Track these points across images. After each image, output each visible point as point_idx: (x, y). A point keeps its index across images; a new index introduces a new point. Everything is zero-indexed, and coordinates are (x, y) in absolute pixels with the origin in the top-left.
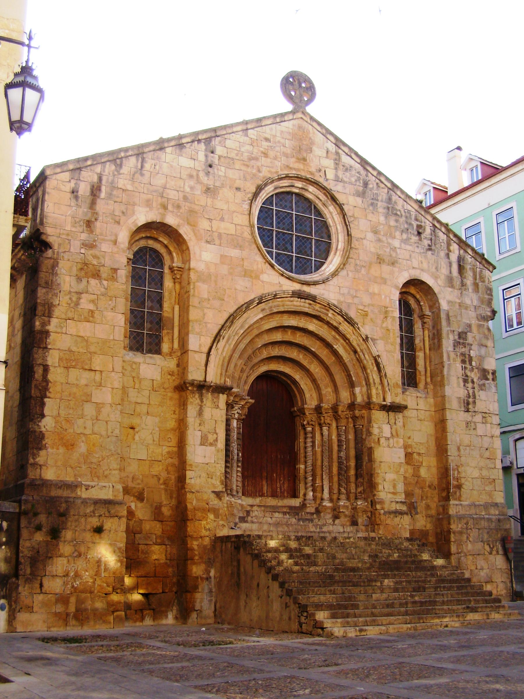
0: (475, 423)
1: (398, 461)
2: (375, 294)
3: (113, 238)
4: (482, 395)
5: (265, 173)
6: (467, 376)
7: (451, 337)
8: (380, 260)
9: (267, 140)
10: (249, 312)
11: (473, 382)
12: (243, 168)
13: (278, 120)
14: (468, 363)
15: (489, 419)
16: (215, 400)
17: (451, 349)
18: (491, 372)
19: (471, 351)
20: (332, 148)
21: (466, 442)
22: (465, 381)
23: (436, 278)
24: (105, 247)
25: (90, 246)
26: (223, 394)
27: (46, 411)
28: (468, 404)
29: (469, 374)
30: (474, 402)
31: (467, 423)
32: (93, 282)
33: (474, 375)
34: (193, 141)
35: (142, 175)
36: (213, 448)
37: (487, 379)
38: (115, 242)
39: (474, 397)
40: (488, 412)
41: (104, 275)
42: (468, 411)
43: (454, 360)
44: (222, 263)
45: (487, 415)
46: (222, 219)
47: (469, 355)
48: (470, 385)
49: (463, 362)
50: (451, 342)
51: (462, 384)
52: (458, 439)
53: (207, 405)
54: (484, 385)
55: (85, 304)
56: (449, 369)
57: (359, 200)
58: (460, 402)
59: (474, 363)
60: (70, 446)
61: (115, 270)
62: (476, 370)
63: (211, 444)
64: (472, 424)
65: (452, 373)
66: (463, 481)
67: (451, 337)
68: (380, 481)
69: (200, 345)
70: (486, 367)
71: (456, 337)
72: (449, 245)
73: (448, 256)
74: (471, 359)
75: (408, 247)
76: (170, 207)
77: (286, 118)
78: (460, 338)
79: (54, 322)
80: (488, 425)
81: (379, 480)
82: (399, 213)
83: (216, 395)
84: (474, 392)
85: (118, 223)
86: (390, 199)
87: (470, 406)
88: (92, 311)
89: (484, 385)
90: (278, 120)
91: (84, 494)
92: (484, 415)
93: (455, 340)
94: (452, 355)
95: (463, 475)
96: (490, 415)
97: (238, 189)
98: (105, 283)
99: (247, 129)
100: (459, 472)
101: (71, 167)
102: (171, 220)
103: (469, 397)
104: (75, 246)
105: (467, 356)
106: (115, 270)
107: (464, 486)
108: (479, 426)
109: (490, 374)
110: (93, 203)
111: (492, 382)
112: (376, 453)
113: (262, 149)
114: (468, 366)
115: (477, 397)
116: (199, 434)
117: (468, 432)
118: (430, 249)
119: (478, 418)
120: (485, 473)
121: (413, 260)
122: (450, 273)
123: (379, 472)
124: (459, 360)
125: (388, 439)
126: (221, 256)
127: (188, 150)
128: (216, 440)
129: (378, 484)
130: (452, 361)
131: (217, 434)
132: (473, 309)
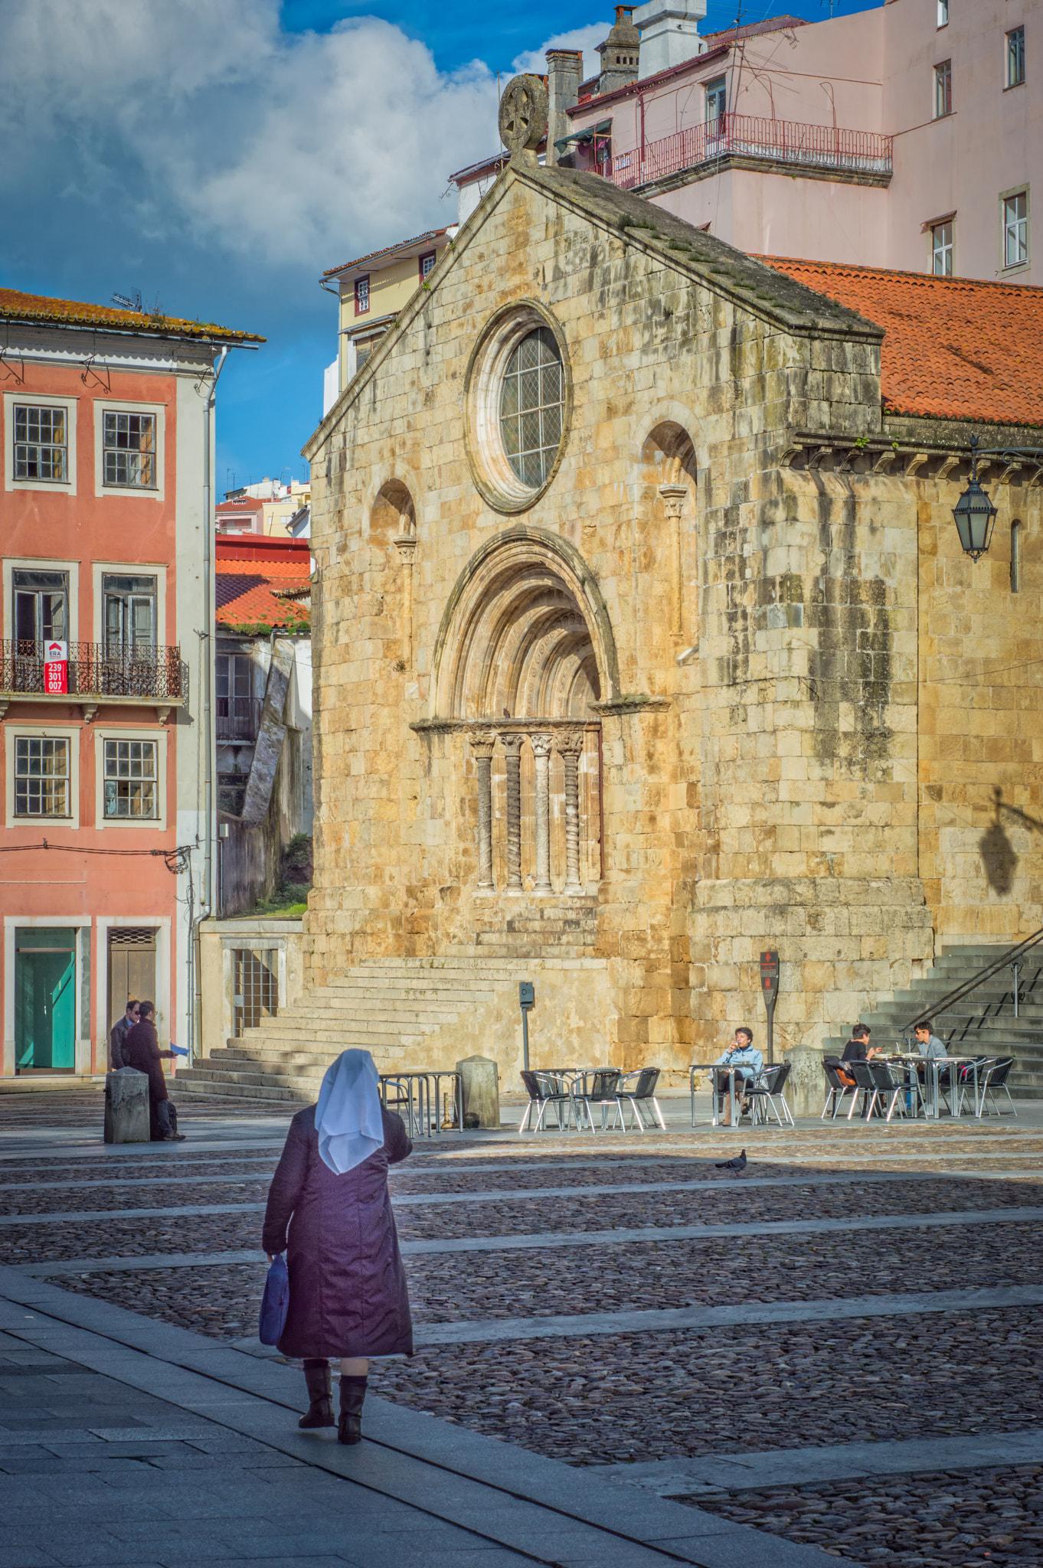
0: (745, 706)
1: (632, 808)
2: (605, 486)
3: (356, 528)
4: (760, 639)
5: (481, 326)
6: (735, 605)
8: (611, 411)
9: (481, 257)
10: (467, 589)
11: (745, 616)
12: (458, 332)
13: (489, 208)
14: (737, 575)
15: (771, 693)
18: (778, 580)
19: (746, 546)
20: (551, 209)
21: (730, 753)
22: (732, 618)
23: (692, 402)
25: (343, 549)
27: (323, 799)
28: (735, 667)
30: (746, 661)
31: (733, 710)
32: (347, 600)
33: (748, 600)
34: (412, 320)
35: (375, 410)
37: (771, 600)
38: (360, 532)
39: (746, 645)
40: (769, 675)
41: (355, 587)
42: (735, 684)
44: (443, 517)
45: (768, 684)
46: (441, 442)
47: (741, 556)
48: (739, 625)
49: (730, 575)
51: (726, 625)
52: (716, 748)
54: (764, 615)
55: (344, 639)
57: (584, 298)
58: (721, 668)
59: (748, 573)
61: (361, 574)
63: (441, 816)
64: (741, 711)
66: (724, 837)
67: (712, 528)
70: (770, 573)
71: (721, 523)
72: (716, 309)
73: (714, 338)
74: (743, 561)
75: (651, 358)
76: (398, 451)
77: (497, 197)
78: (726, 524)
79: (323, 670)
80: (769, 707)
82: (639, 289)
84: (746, 636)
85: (360, 501)
86: (627, 266)
87: (739, 673)
88: (347, 645)
89: (764, 615)
90: (489, 208)
92: (762, 685)
93: (718, 531)
95: (722, 823)
96: (773, 682)
97: (454, 376)
98: (356, 597)
99: (460, 255)
100: (717, 819)
101: (322, 437)
102: (401, 471)
103: (737, 653)
105: (737, 560)
106: (361, 574)
108: (752, 711)
109: (778, 588)
110: (341, 483)
111: (779, 605)
113: (476, 281)
114: (738, 583)
115: (752, 648)
118: (687, 341)
119: (752, 695)
120: (762, 815)
121: (660, 383)
122: (717, 378)
125: (620, 768)
126: (443, 504)
127: (410, 339)
130: (710, 578)
132: (752, 446)
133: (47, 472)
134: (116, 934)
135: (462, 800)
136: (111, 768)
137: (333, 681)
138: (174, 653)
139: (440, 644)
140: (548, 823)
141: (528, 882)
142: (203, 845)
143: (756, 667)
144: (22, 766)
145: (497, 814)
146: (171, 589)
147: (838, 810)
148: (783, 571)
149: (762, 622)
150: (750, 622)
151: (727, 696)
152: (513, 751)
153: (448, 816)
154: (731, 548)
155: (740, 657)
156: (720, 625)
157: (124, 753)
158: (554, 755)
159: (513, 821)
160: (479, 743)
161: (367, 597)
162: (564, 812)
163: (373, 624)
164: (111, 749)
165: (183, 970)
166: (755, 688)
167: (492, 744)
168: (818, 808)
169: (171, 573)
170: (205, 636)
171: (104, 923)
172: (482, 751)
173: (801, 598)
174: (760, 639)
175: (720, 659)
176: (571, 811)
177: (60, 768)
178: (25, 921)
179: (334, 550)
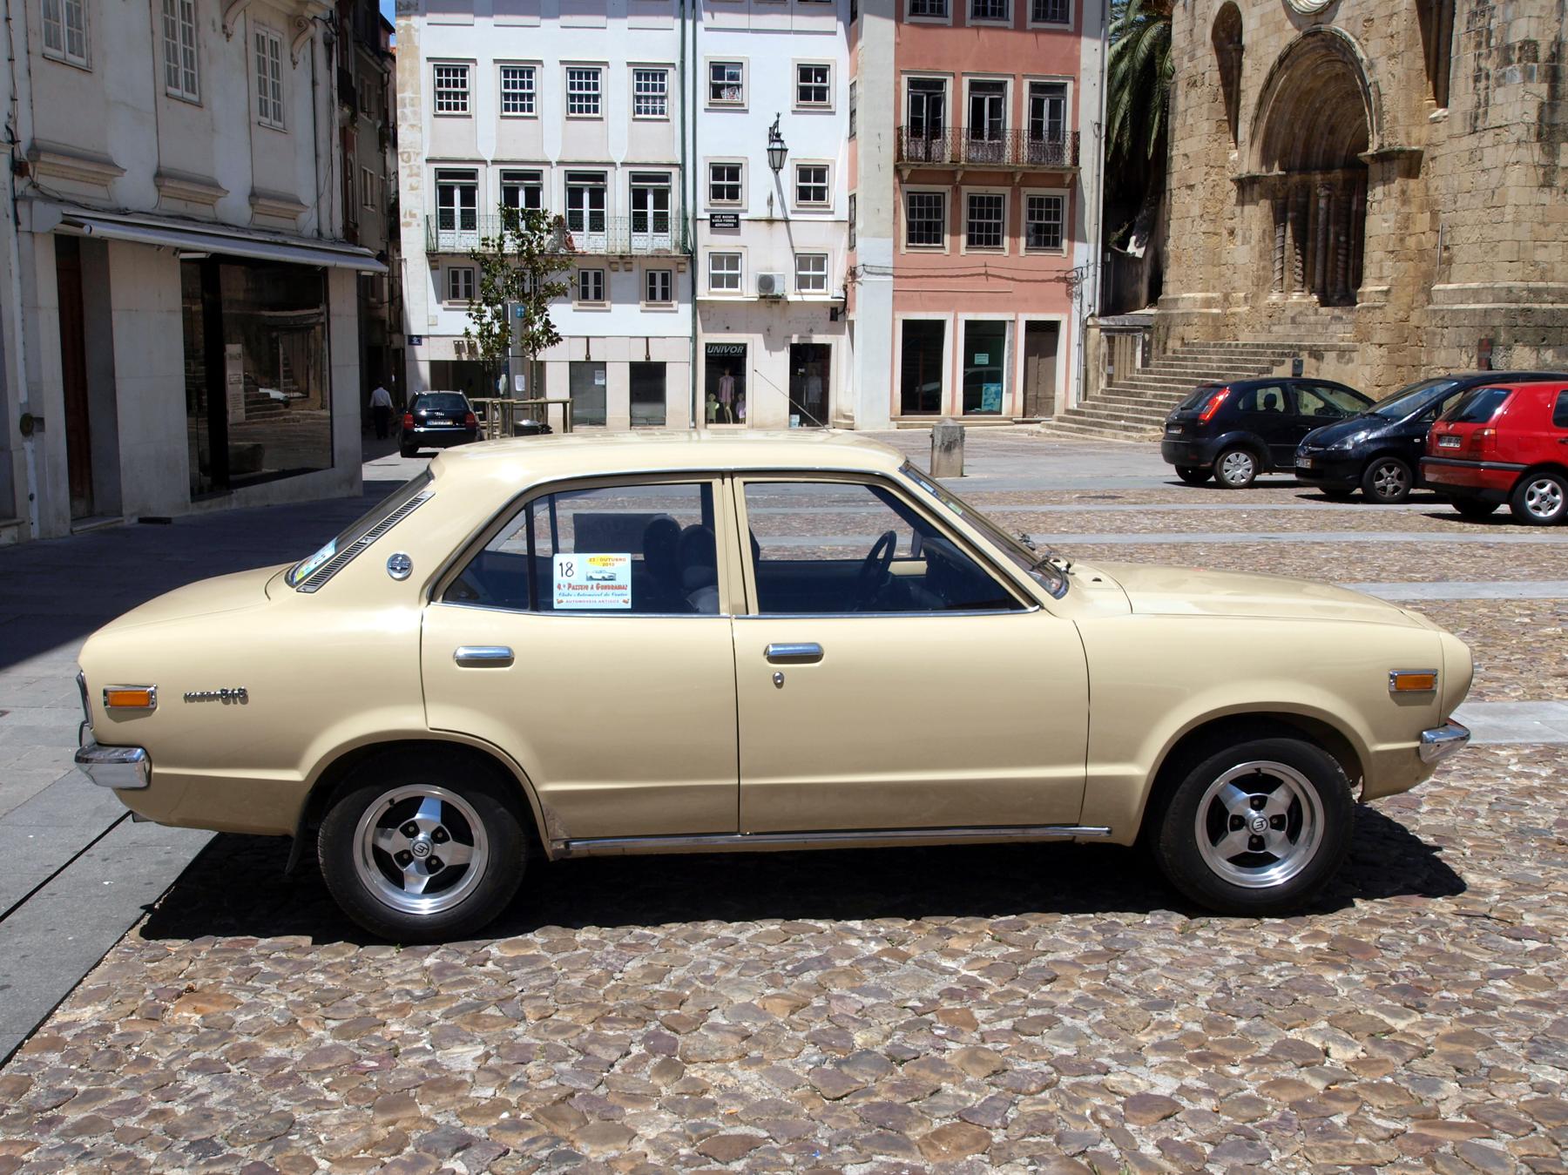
4: (1499, 95)
6: (1480, 70)
7: (1466, 8)
17: (1464, 30)
22: (1477, 79)
24: (1199, 53)
28: (1476, 118)
29: (1483, 64)
30: (1486, 113)
37: (1510, 62)
39: (1487, 101)
42: (1475, 132)
43: (1466, 47)
48: (1482, 85)
49: (1478, 45)
50: (1465, 17)
54: (1504, 75)
55: (1190, 121)
56: (1457, 67)
60: (1179, 259)
62: (1495, 53)
65: (1461, 73)
74: (1490, 32)
80: (1502, 147)
81: (1366, 261)
89: (1504, 75)
91: (1182, 308)
94: (1464, 39)
103: (1478, 107)
104: (1186, 64)
107: (1457, 259)
112: (1367, 224)
114: (1484, 51)
117: (1472, 168)
119: (1489, 138)
124: (1473, 44)
133: (993, 13)
134: (1031, 327)
136: (1031, 216)
137: (1182, 151)
138: (1076, 135)
139: (1256, 118)
140: (1326, 246)
142: (1091, 269)
143: (1494, 118)
144: (972, 215)
146: (1076, 91)
147: (1553, 228)
148: (1522, 38)
149: (1501, 81)
150: (1492, 82)
151: (1469, 142)
154: (1480, 23)
155: (1481, 110)
156: (1467, 88)
157: (1040, 206)
161: (1206, 89)
163: (1210, 109)
164: (1032, 202)
165: (1075, 351)
166: (1491, 133)
168: (1536, 227)
169: (1076, 80)
170: (1100, 126)
171: (1023, 318)
173: (1535, 60)
174: (1499, 95)
175: (1465, 113)
177: (998, 216)
178: (972, 317)
179: (1186, 58)
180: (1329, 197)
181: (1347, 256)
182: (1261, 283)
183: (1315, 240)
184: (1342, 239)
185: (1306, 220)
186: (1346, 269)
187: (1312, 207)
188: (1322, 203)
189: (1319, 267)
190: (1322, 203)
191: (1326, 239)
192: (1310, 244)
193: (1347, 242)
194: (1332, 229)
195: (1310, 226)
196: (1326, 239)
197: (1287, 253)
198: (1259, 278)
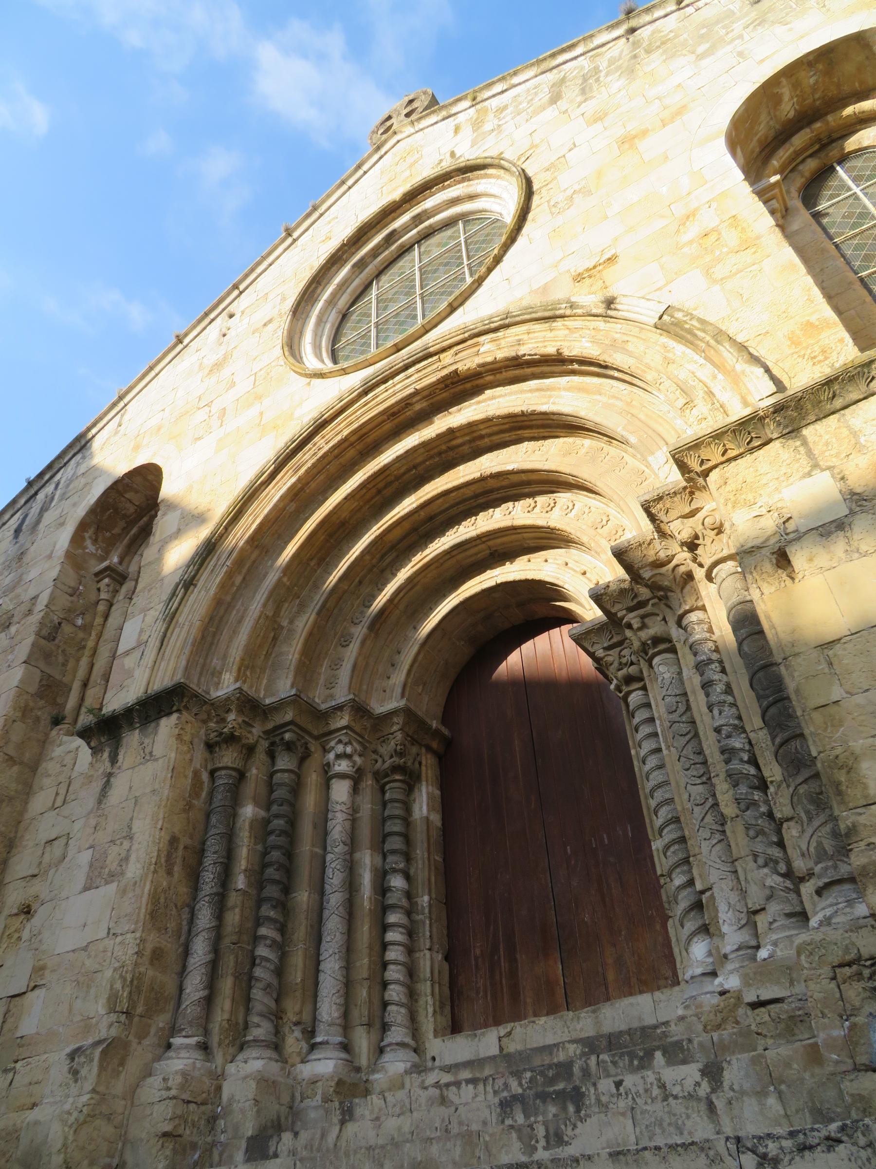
16: (146, 741)
26: (169, 714)
36: (113, 887)
38: (50, 557)
53: (124, 767)
68: (858, 744)
69: (142, 631)
83: (153, 725)
101: (22, 501)
116: (85, 857)
123: (837, 693)
128: (127, 859)
129: (848, 765)
131: (131, 838)
135: (173, 841)
141: (293, 1041)
145: (240, 882)
152: (284, 762)
153: (133, 870)
158: (368, 782)
159: (272, 891)
160: (231, 739)
162: (382, 889)
167: (250, 750)
172: (229, 757)
176: (397, 882)
180: (356, 779)
181: (411, 933)
182: (146, 1007)
183: (320, 890)
184: (397, 882)
185: (291, 832)
186: (411, 972)
187: (310, 801)
188: (341, 791)
189: (331, 967)
190: (341, 791)
191: (351, 886)
192: (303, 897)
193: (409, 895)
194: (367, 859)
195: (306, 847)
196: (351, 886)
197: (233, 918)
198: (135, 985)
